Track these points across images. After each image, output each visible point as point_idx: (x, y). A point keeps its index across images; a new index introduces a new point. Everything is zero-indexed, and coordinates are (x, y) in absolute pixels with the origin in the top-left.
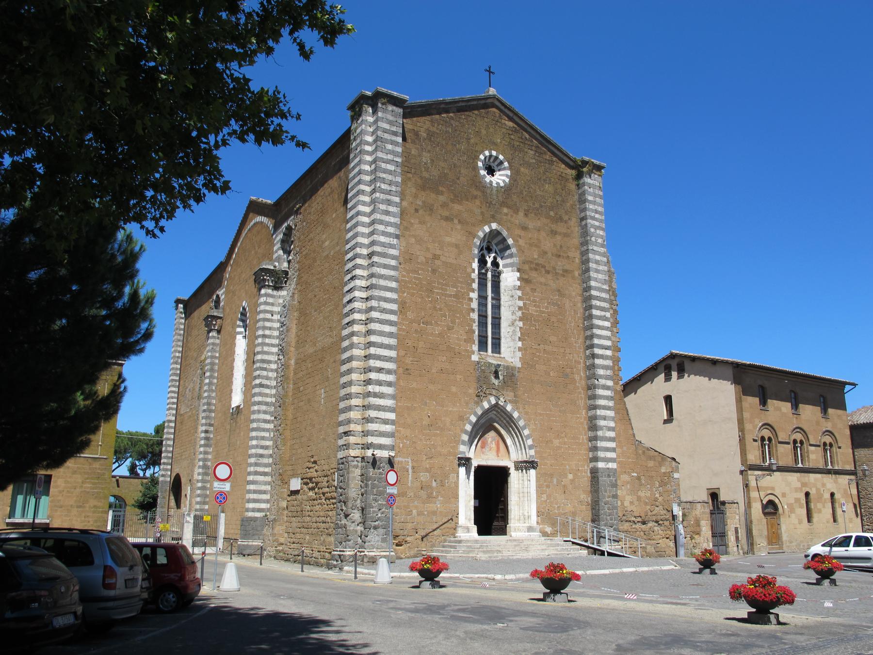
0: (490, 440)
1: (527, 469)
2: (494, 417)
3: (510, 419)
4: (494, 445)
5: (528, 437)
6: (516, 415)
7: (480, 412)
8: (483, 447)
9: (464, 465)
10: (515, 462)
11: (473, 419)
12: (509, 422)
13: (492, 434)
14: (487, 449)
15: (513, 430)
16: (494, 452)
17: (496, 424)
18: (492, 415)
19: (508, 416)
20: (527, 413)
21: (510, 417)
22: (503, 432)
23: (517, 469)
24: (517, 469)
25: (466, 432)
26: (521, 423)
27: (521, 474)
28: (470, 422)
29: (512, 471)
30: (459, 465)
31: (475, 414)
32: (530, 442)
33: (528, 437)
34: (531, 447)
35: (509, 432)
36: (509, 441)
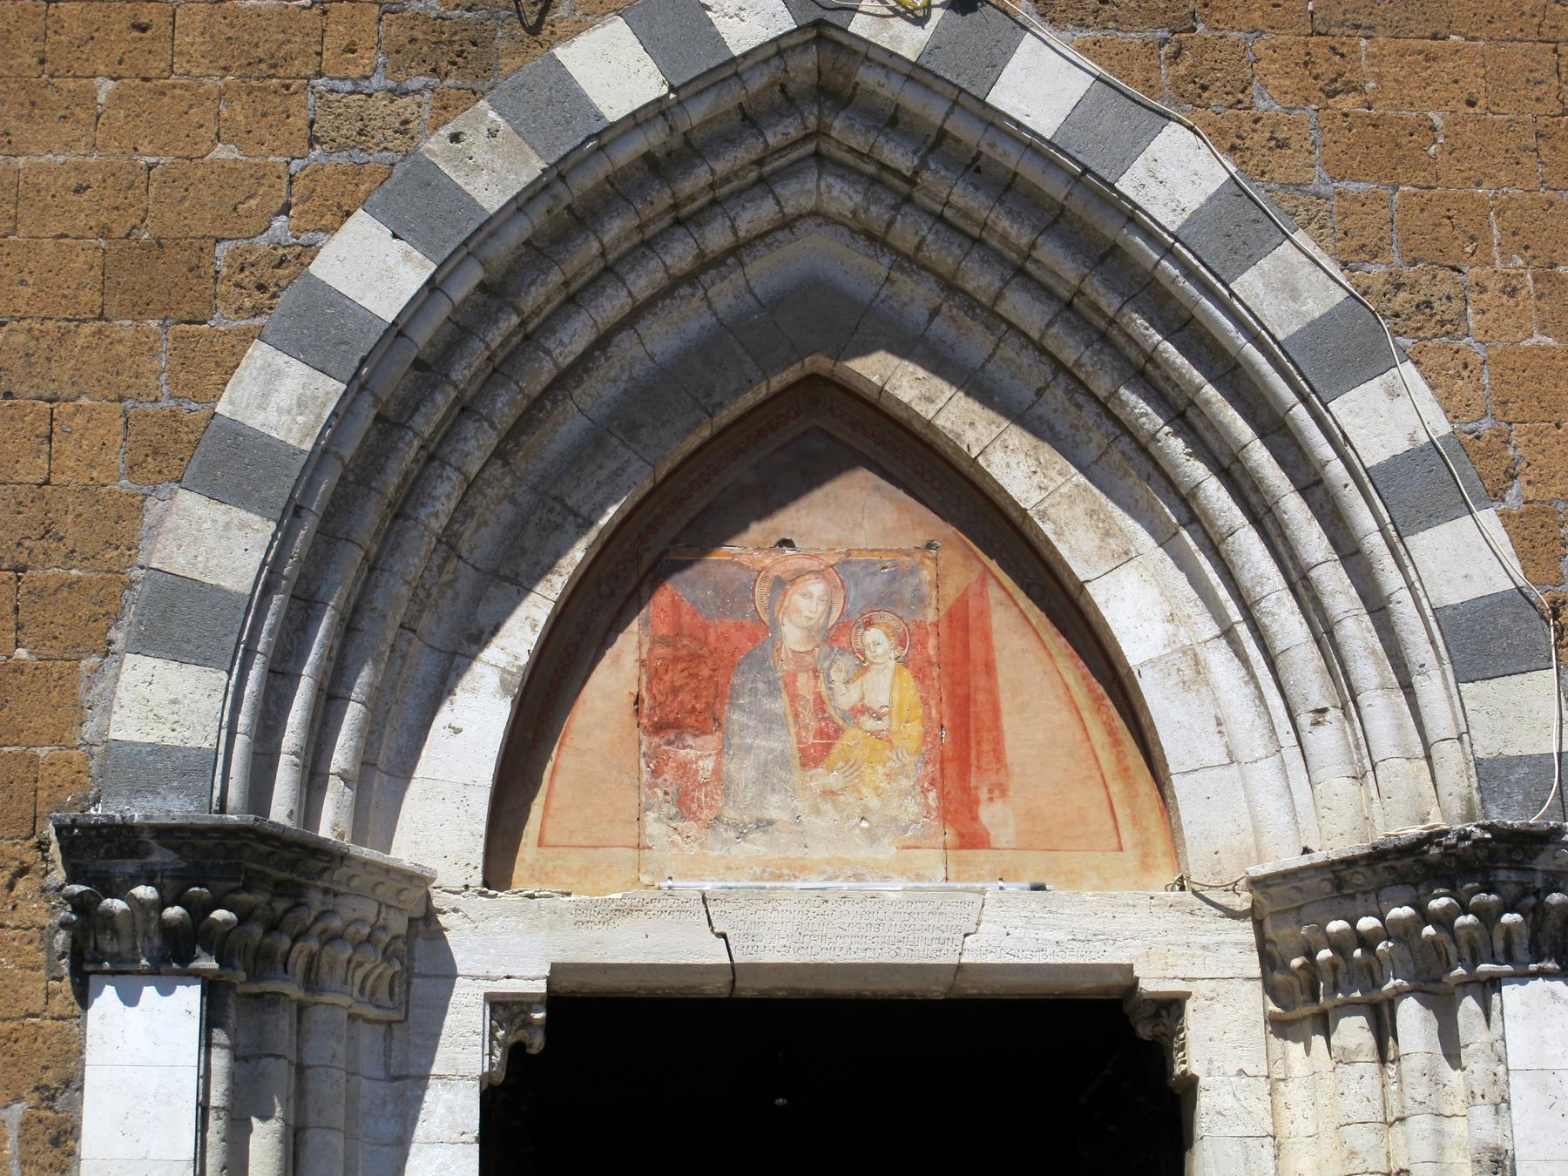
0: (805, 609)
1: (1452, 978)
2: (858, 269)
3: (1107, 258)
4: (883, 682)
5: (1423, 488)
6: (1174, 175)
7: (491, 166)
8: (682, 707)
9: (170, 957)
10: (1286, 908)
11: (374, 270)
12: (1109, 330)
13: (854, 517)
14: (756, 738)
15: (1184, 416)
16: (894, 784)
17: (905, 383)
18: (813, 232)
19: (1055, 220)
20: (1385, 146)
21: (1070, 208)
22: (1019, 468)
23: (1301, 1000)
24: (1301, 1000)
25: (231, 463)
26: (1288, 289)
27: (1362, 1081)
28: (318, 327)
29: (1225, 1045)
30: (94, 956)
31: (415, 204)
32: (1466, 558)
33: (1423, 488)
34: (1482, 642)
35: (1127, 470)
36: (1141, 600)
